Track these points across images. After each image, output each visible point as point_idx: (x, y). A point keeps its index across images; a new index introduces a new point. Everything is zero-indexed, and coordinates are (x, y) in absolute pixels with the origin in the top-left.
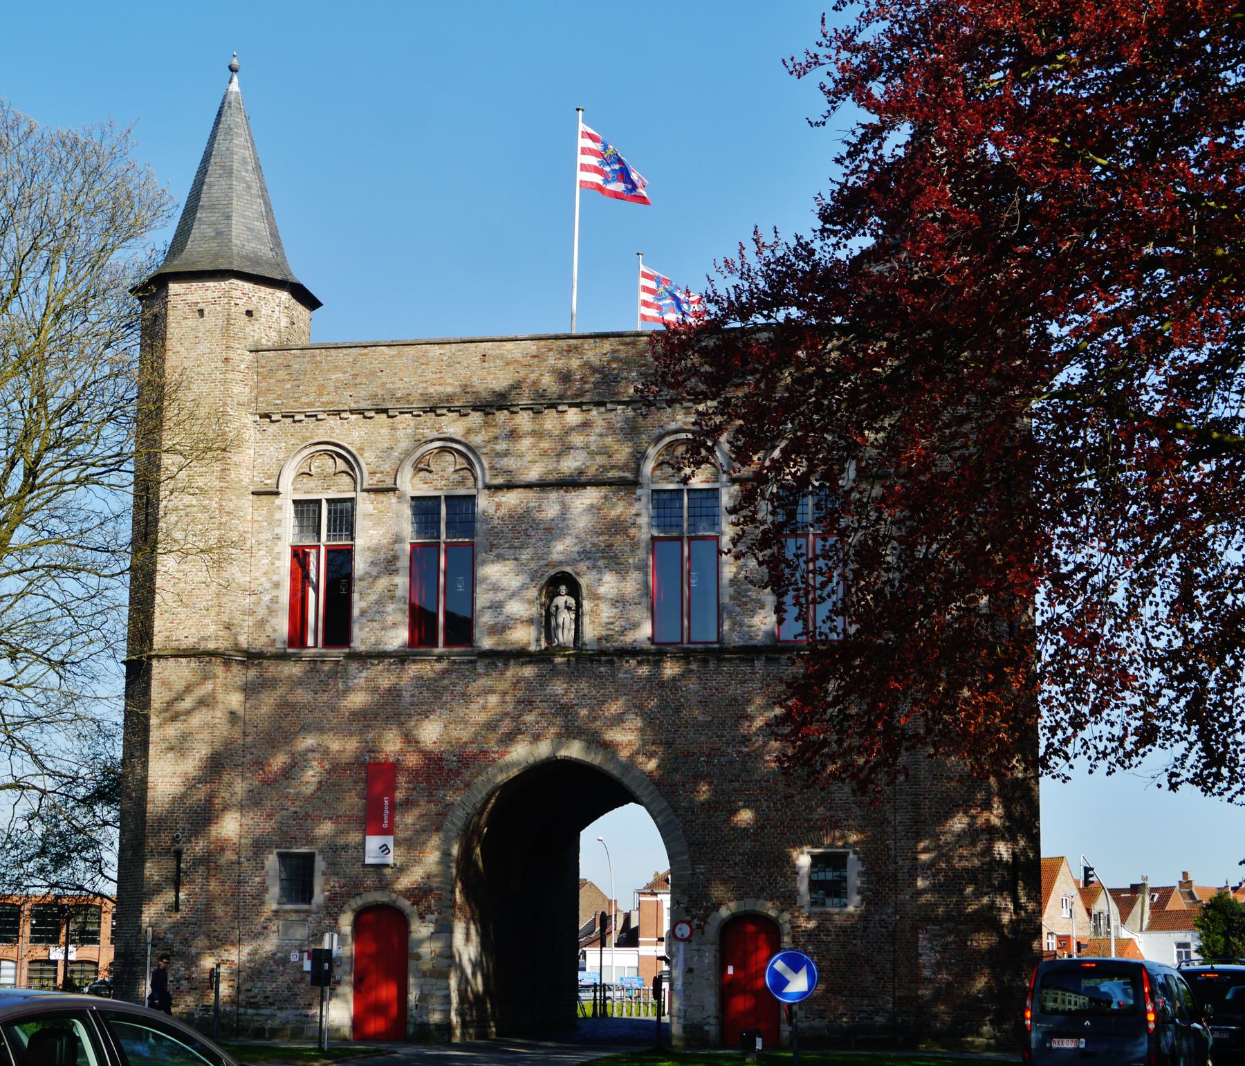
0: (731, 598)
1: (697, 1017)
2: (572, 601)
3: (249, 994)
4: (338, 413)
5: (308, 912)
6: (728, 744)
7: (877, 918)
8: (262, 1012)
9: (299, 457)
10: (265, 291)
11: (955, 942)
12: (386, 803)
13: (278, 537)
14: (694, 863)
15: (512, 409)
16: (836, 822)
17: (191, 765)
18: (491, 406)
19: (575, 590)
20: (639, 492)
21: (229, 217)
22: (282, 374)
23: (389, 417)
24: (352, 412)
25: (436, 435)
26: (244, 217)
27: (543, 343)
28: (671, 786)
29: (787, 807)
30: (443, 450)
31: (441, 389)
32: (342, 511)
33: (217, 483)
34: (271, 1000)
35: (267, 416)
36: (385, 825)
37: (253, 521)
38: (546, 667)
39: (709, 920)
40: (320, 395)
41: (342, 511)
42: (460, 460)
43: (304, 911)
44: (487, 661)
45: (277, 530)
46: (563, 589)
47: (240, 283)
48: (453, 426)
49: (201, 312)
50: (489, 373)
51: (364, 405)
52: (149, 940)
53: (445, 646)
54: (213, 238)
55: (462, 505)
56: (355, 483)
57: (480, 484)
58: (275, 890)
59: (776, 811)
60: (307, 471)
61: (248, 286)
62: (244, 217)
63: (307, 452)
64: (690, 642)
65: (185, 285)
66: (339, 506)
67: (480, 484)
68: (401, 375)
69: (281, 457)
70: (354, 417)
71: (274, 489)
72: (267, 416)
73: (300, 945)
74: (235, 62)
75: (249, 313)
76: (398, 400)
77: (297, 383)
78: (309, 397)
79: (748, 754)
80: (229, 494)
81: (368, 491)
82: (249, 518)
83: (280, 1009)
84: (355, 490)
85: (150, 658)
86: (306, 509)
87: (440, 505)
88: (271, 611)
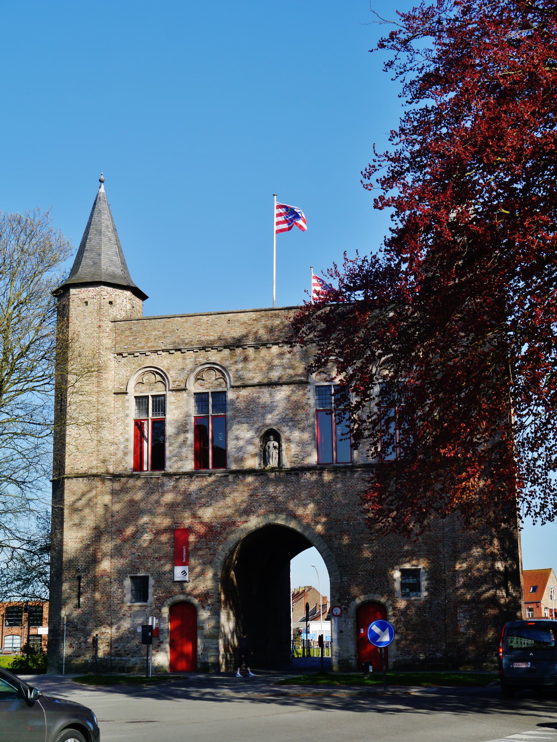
1: (345, 655)
2: (276, 444)
3: (116, 649)
4: (156, 351)
5: (146, 606)
6: (357, 514)
7: (436, 602)
8: (124, 658)
10: (118, 291)
11: (476, 614)
12: (184, 550)
13: (127, 416)
15: (244, 347)
16: (414, 553)
17: (85, 533)
18: (233, 346)
19: (278, 438)
20: (309, 387)
21: (100, 255)
22: (127, 333)
23: (182, 353)
24: (163, 351)
25: (205, 361)
26: (107, 254)
27: (258, 313)
28: (329, 537)
30: (210, 368)
31: (207, 338)
32: (159, 401)
33: (96, 389)
34: (128, 652)
35: (120, 354)
36: (184, 561)
37: (115, 408)
38: (263, 478)
39: (350, 605)
40: (147, 342)
41: (159, 401)
42: (218, 373)
43: (143, 606)
44: (234, 475)
45: (127, 412)
46: (272, 437)
47: (106, 288)
48: (214, 356)
49: (86, 303)
50: (232, 329)
51: (169, 347)
52: (65, 623)
53: (213, 467)
54: (92, 266)
55: (220, 396)
56: (166, 387)
57: (229, 386)
58: (128, 597)
59: (383, 548)
61: (110, 289)
62: (107, 254)
63: (141, 372)
64: (337, 463)
65: (78, 290)
66: (158, 399)
67: (229, 386)
68: (187, 331)
69: (128, 375)
70: (164, 353)
71: (125, 391)
72: (120, 354)
74: (102, 177)
75: (111, 303)
76: (186, 344)
77: (135, 337)
78: (141, 344)
80: (102, 394)
81: (172, 390)
82: (112, 406)
83: (133, 657)
84: (166, 391)
85: (63, 478)
86: (141, 401)
87: (208, 397)
88: (125, 454)
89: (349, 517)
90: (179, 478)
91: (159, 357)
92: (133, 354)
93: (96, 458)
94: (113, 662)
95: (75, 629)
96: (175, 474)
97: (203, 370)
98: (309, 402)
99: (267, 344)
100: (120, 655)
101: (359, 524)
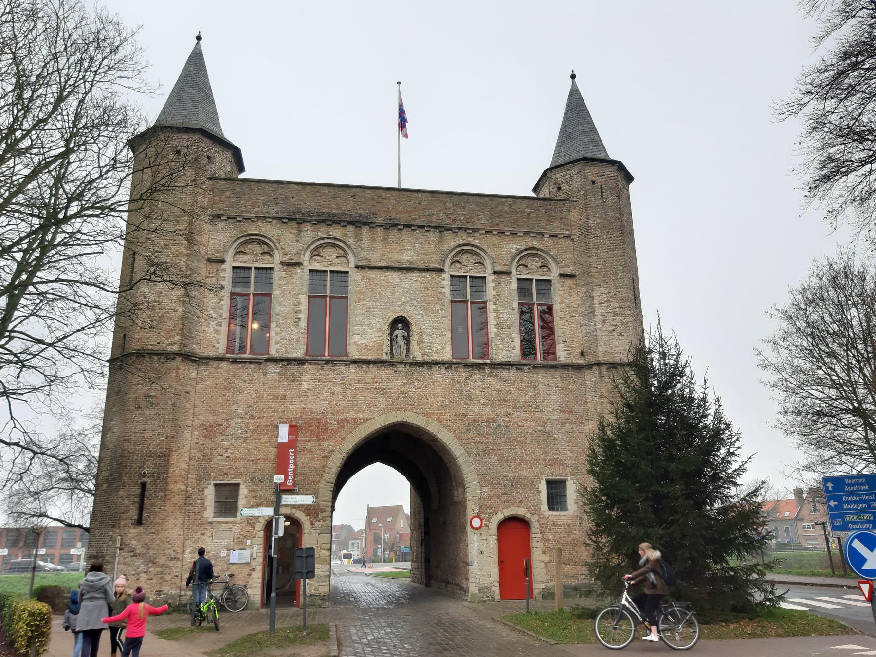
0: (496, 335)
2: (406, 334)
6: (498, 416)
9: (238, 242)
20: (443, 275)
22: (229, 193)
24: (274, 218)
29: (532, 452)
30: (329, 244)
33: (185, 251)
39: (491, 521)
42: (341, 251)
43: (231, 522)
49: (178, 152)
50: (357, 205)
51: (281, 215)
61: (209, 142)
70: (274, 222)
72: (219, 216)
75: (209, 157)
76: (303, 214)
79: (509, 422)
80: (192, 258)
89: (489, 419)
90: (287, 365)
91: (267, 225)
92: (235, 218)
93: (180, 332)
94: (183, 598)
95: (132, 554)
96: (282, 360)
97: (321, 246)
98: (444, 291)
99: (399, 225)
101: (499, 426)
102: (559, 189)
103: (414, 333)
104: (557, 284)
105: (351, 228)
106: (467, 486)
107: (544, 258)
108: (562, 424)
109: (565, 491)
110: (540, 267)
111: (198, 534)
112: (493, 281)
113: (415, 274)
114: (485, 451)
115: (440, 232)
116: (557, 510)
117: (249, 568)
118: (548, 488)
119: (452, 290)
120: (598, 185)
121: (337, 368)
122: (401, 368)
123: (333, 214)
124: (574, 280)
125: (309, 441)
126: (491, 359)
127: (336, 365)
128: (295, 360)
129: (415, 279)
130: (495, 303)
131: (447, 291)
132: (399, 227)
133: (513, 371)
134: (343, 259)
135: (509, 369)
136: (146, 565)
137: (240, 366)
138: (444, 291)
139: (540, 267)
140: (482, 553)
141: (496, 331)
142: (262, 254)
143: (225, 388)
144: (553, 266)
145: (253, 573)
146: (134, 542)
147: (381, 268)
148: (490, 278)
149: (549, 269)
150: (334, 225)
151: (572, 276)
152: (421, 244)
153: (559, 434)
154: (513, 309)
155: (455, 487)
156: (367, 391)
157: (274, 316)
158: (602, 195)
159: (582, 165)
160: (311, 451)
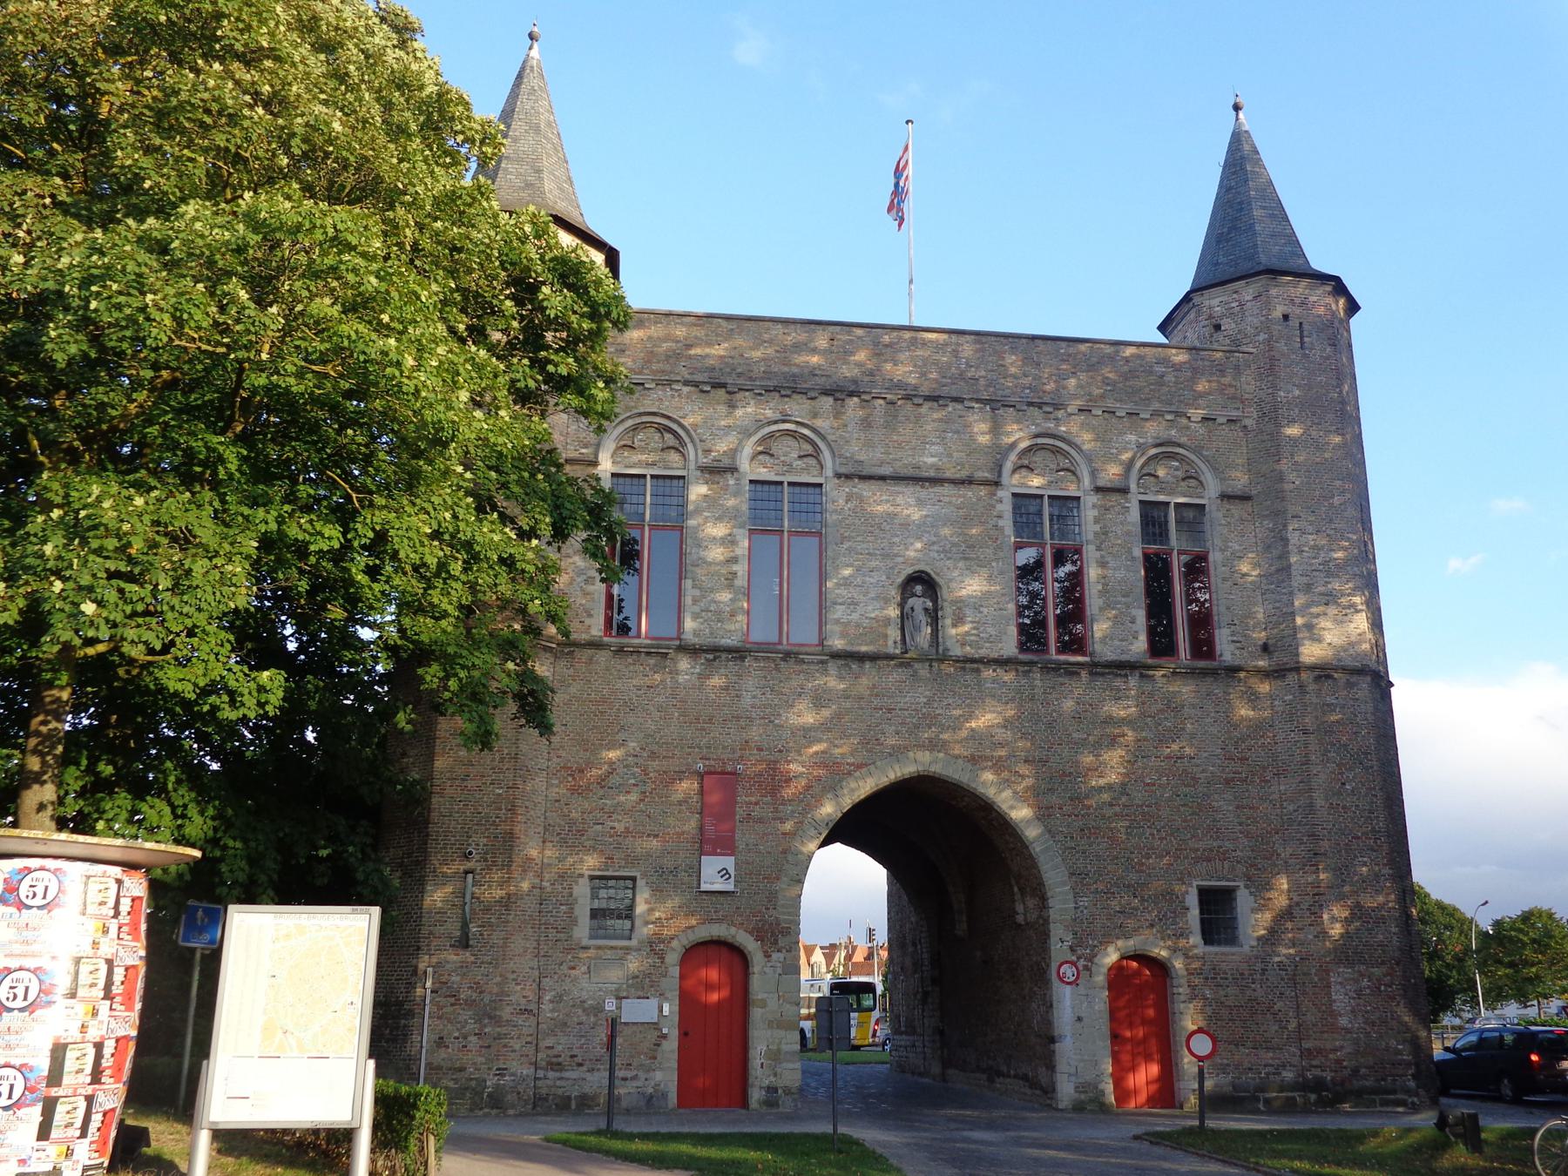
11: (1369, 987)
14: (1076, 895)
15: (863, 397)
20: (1000, 493)
21: (539, 171)
24: (686, 383)
25: (778, 416)
28: (1047, 808)
29: (1172, 835)
34: (579, 1059)
44: (841, 662)
51: (698, 377)
54: (523, 189)
59: (1161, 839)
60: (630, 443)
70: (686, 389)
73: (617, 990)
76: (740, 375)
83: (591, 1070)
90: (714, 659)
91: (673, 396)
97: (771, 435)
98: (1001, 523)
100: (555, 1066)
102: (1217, 327)
103: (945, 604)
104: (1217, 514)
105: (828, 402)
106: (1049, 894)
107: (1190, 463)
108: (1227, 782)
109: (1233, 909)
110: (1183, 479)
111: (564, 967)
112: (1094, 506)
113: (947, 490)
114: (1082, 830)
115: (993, 409)
116: (1219, 943)
117: (657, 1033)
118: (1201, 902)
119: (1015, 522)
120: (1294, 323)
121: (805, 667)
122: (923, 670)
123: (794, 375)
124: (1248, 506)
125: (756, 804)
126: (1091, 655)
127: (803, 661)
128: (729, 650)
129: (947, 499)
130: (1099, 549)
131: (1007, 524)
132: (916, 401)
133: (1133, 681)
134: (812, 461)
135: (1126, 676)
136: (479, 1021)
137: (630, 660)
138: (1001, 523)
139: (1183, 479)
140: (1079, 1019)
141: (1100, 602)
142: (663, 450)
143: (604, 701)
144: (1208, 477)
145: (664, 1042)
146: (456, 979)
147: (883, 478)
148: (1090, 501)
149: (1201, 482)
150: (795, 396)
151: (1245, 498)
152: (957, 432)
153: (1223, 803)
154: (1133, 559)
155: (1018, 896)
156: (860, 712)
157: (689, 568)
158: (1302, 343)
159: (1264, 282)
160: (761, 821)
